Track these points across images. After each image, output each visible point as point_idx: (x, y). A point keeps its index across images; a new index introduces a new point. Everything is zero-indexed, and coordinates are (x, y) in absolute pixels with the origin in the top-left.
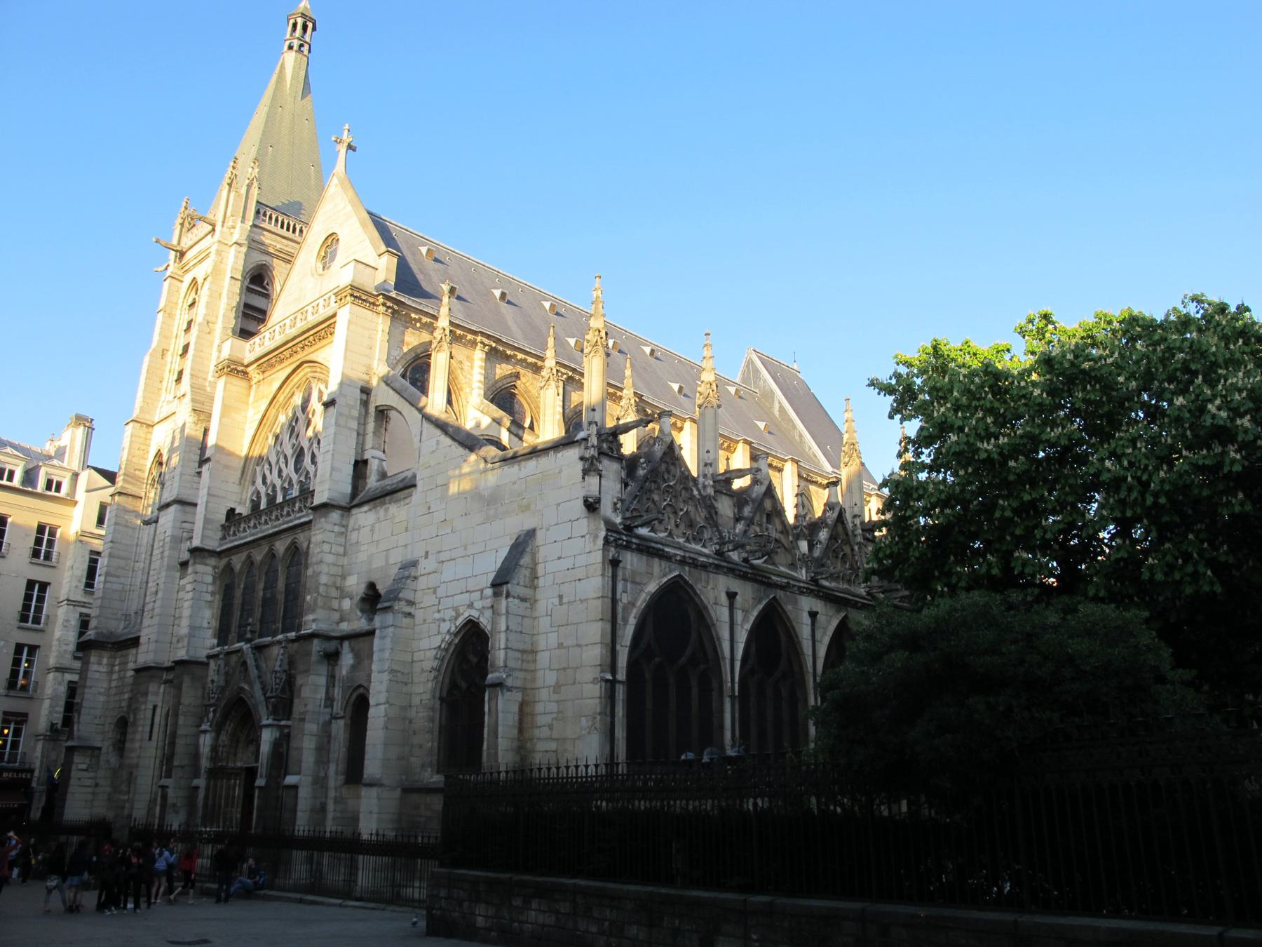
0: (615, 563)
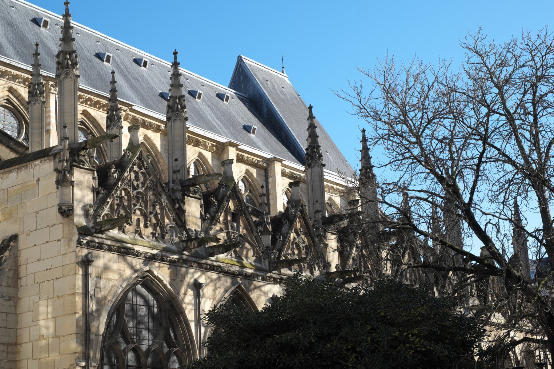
0: (86, 263)
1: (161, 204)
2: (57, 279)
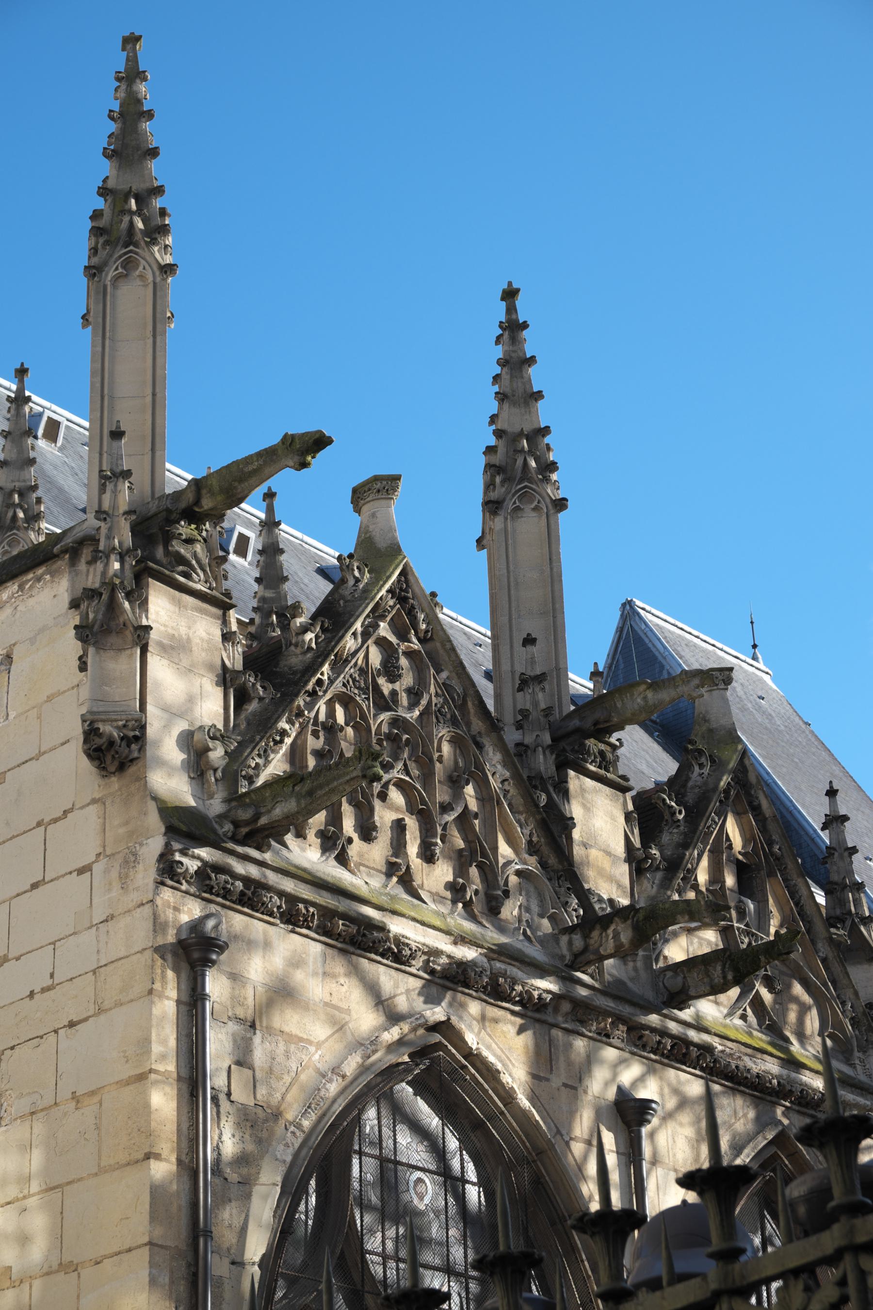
0: (195, 952)
1: (482, 785)
2: (72, 1024)
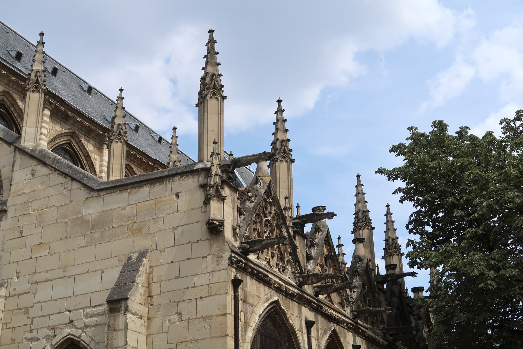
0: (236, 283)
